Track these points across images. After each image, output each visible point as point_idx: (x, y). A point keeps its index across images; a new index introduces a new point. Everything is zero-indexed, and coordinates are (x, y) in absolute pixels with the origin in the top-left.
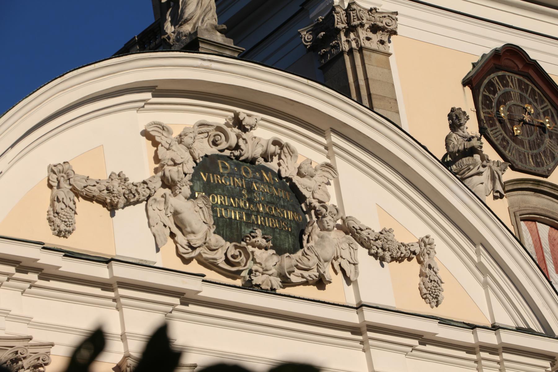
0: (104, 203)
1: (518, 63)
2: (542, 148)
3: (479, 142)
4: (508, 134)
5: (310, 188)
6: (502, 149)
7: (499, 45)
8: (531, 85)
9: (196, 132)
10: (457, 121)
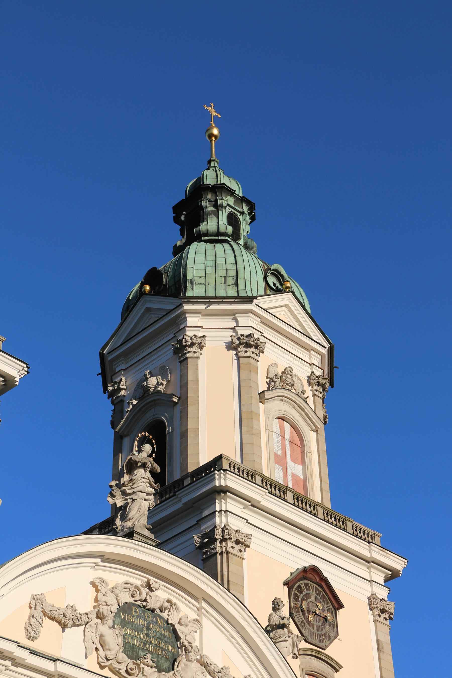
0: (60, 623)
1: (317, 577)
2: (324, 631)
3: (288, 621)
4: (306, 618)
5: (184, 633)
6: (301, 628)
7: (307, 565)
8: (323, 592)
9: (123, 587)
10: (277, 606)
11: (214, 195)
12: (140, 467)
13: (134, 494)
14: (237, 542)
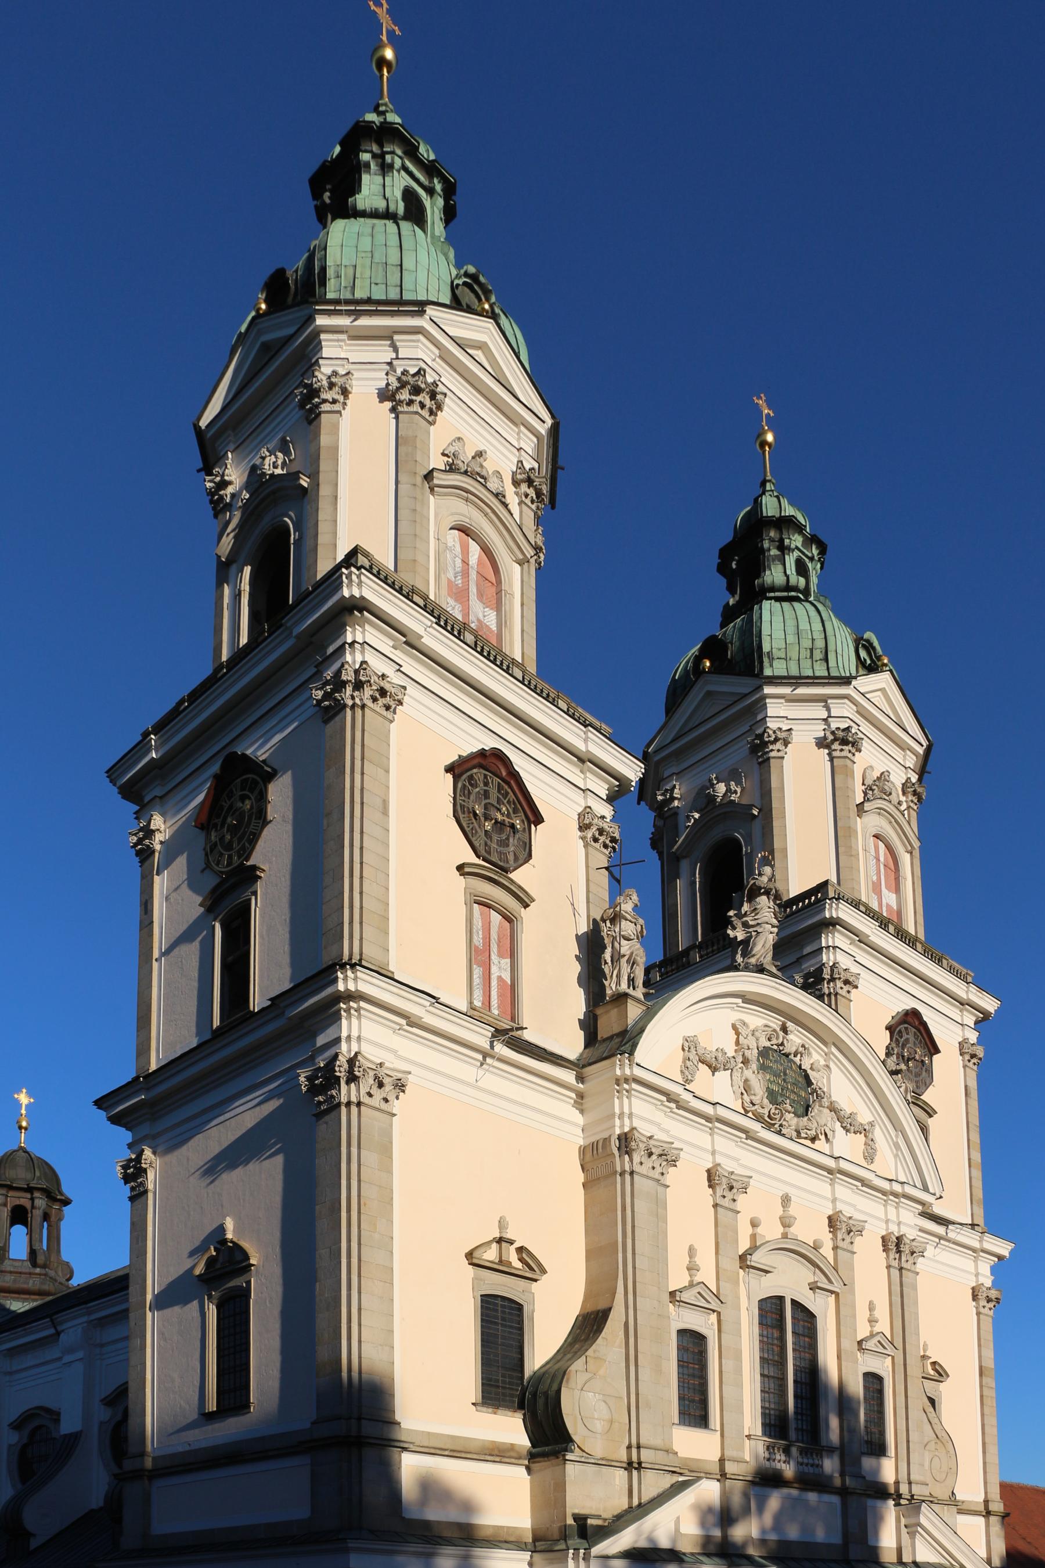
0: (710, 1066)
1: (915, 1021)
7: (908, 1008)
8: (920, 1036)
11: (778, 532)
12: (763, 894)
13: (759, 927)
14: (847, 982)
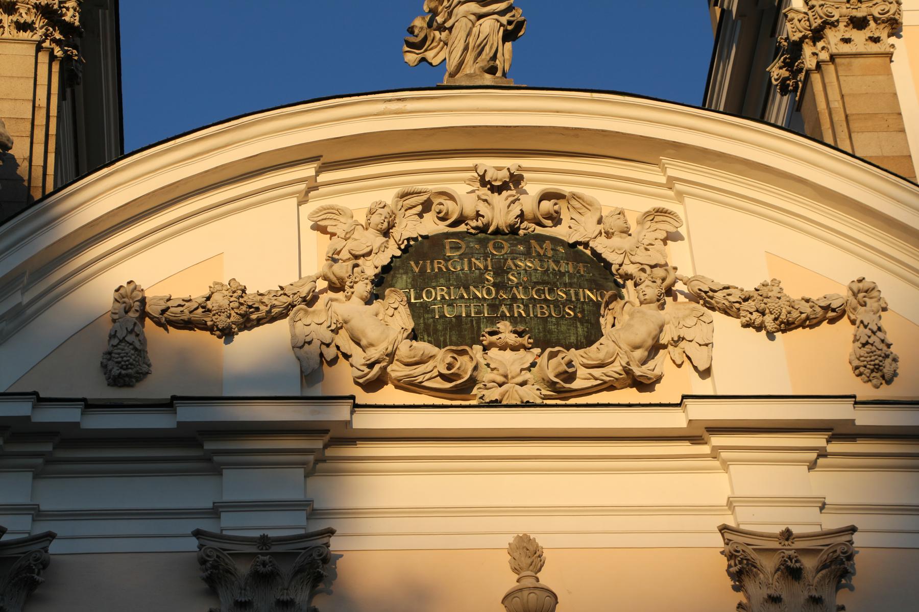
5: (619, 250)
